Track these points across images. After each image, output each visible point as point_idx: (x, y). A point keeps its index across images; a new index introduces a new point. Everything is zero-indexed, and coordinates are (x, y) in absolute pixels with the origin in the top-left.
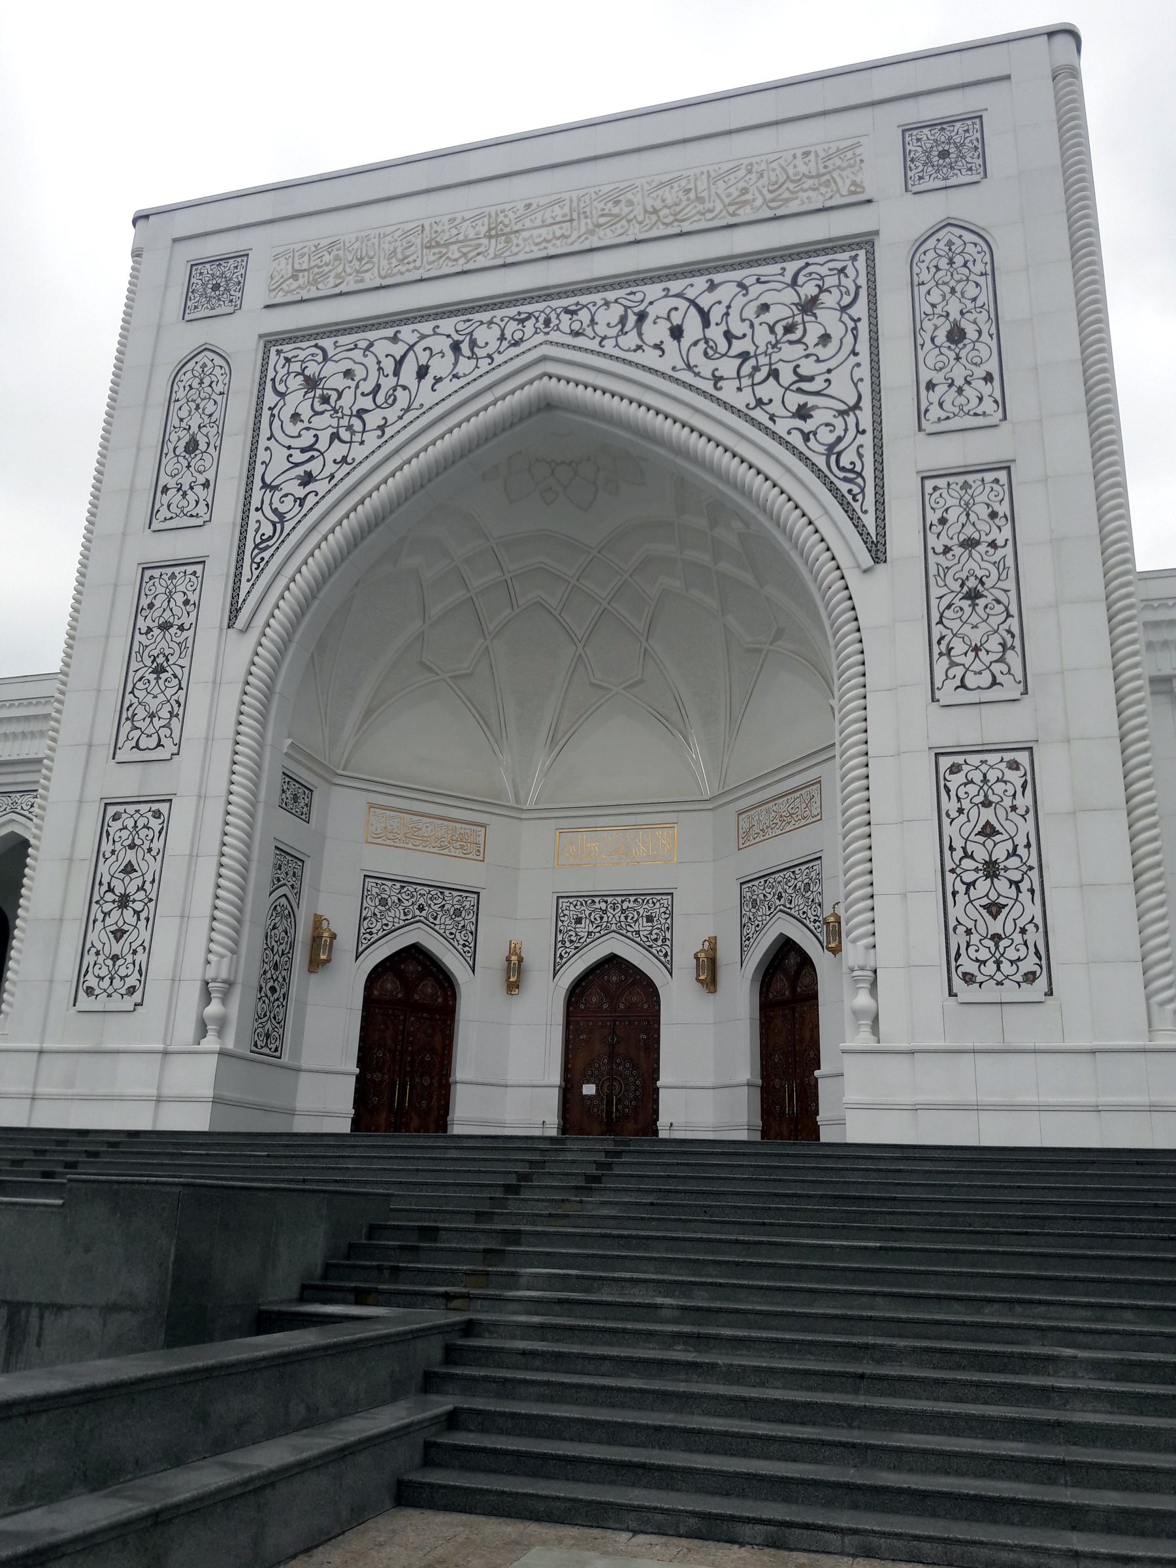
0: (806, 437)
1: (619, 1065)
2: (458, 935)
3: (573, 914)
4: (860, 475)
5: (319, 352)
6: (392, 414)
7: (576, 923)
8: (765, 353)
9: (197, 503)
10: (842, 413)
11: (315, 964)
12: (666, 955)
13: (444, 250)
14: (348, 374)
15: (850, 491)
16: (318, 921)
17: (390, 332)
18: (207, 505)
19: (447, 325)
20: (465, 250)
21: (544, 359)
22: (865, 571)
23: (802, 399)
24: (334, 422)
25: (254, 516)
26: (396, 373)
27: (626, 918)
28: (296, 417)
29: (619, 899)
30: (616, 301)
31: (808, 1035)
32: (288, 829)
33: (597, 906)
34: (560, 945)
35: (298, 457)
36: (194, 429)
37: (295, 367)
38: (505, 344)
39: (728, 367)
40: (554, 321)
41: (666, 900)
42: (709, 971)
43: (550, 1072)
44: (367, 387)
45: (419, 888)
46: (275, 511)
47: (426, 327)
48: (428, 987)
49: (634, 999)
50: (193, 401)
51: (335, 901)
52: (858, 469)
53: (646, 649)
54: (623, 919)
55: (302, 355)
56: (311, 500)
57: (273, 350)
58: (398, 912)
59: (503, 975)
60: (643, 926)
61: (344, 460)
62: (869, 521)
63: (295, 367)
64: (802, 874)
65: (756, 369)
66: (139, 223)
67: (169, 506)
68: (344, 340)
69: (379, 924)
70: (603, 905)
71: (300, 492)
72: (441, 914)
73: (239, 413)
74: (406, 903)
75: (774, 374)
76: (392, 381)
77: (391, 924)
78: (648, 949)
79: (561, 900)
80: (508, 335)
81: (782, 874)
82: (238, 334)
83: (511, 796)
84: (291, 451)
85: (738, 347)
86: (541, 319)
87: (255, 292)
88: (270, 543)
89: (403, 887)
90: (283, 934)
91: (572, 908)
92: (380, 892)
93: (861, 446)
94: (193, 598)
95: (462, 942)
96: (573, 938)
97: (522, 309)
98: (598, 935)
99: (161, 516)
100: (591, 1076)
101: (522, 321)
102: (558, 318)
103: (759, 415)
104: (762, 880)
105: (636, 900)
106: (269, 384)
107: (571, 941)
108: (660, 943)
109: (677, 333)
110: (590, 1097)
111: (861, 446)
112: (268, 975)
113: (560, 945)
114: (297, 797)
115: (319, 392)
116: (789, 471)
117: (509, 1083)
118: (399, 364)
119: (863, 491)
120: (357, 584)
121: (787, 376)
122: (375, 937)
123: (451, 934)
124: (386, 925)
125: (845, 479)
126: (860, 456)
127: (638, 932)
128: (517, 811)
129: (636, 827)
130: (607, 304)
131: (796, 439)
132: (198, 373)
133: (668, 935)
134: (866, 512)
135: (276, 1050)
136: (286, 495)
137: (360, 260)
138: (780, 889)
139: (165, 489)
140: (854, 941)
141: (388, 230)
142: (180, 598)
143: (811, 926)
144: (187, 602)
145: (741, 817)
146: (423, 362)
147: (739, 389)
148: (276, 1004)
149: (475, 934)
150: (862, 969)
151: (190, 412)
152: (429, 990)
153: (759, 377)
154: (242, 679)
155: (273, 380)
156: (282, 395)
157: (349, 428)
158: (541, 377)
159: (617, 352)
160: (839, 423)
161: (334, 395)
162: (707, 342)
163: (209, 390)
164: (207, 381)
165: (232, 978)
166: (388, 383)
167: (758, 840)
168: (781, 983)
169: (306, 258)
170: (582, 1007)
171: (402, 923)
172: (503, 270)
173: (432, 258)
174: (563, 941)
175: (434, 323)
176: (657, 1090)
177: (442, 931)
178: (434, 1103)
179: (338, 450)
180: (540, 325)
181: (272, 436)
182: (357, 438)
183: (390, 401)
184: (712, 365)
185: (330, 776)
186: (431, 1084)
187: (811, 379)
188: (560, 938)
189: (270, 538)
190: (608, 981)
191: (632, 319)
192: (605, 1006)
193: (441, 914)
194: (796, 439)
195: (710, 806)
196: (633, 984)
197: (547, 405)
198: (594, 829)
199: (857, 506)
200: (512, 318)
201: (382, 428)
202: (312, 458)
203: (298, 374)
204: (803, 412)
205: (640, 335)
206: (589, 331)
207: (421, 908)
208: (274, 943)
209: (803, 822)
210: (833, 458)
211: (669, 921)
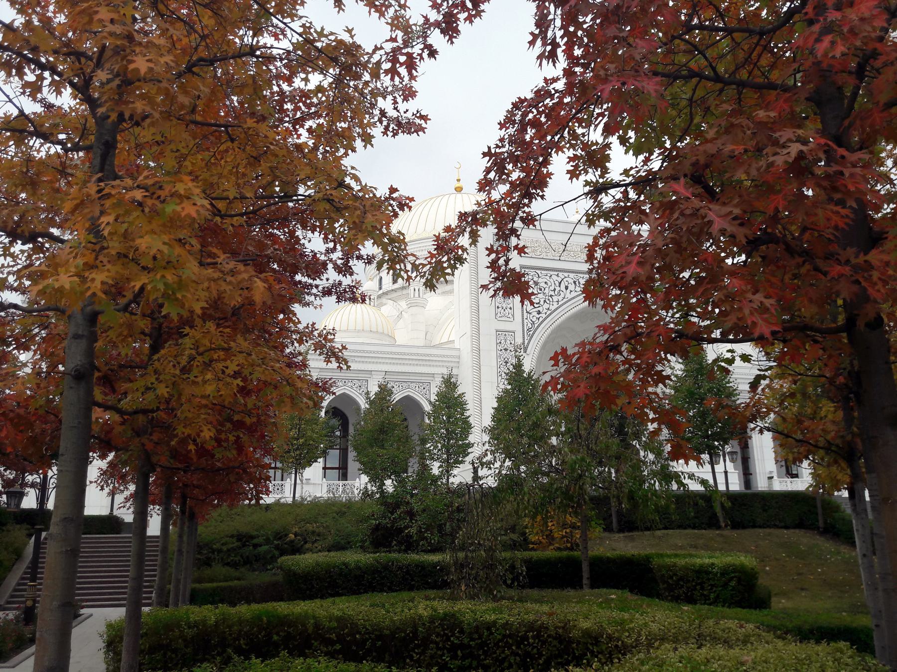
6: (560, 298)
19: (572, 275)
25: (526, 321)
47: (566, 275)
56: (541, 319)
118: (560, 283)
179: (546, 306)
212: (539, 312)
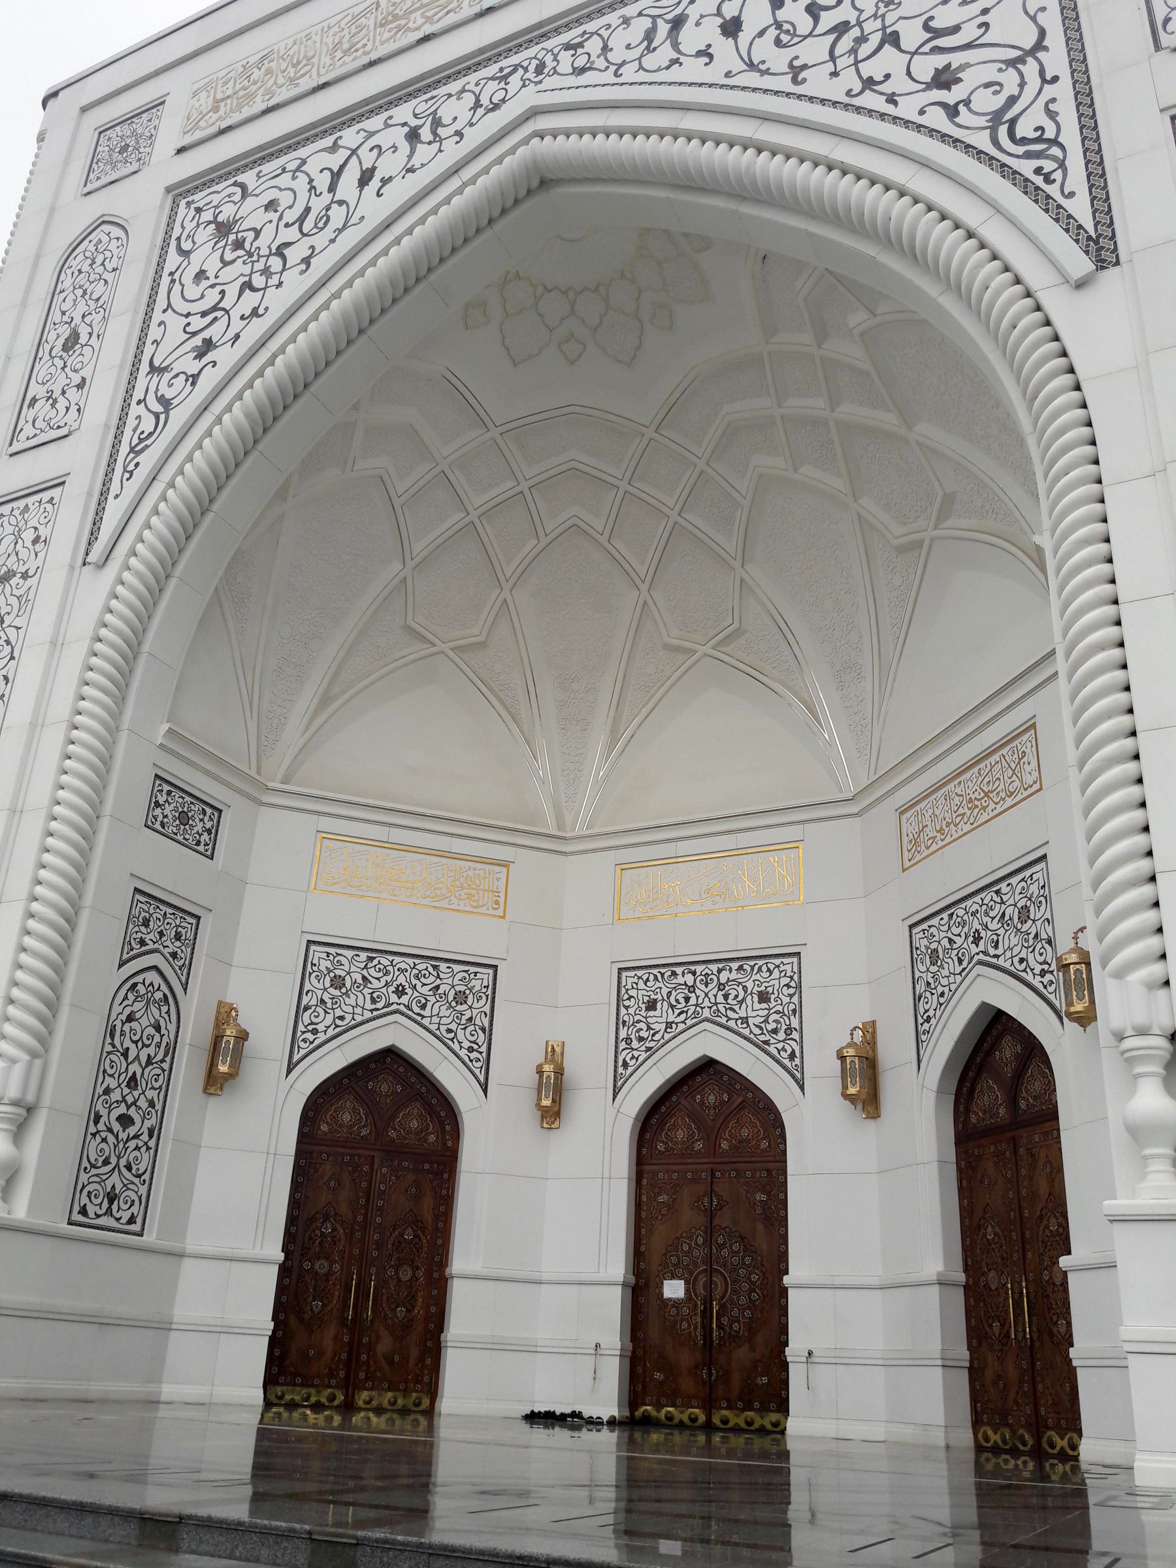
0: (952, 111)
1: (721, 1247)
2: (460, 1033)
3: (642, 994)
4: (1055, 142)
5: (238, 190)
6: (320, 240)
7: (648, 1009)
8: (875, 16)
9: (68, 409)
10: (1012, 63)
11: (213, 1082)
12: (792, 1056)
13: (403, 22)
14: (271, 206)
15: (1038, 171)
16: (225, 1014)
17: (328, 141)
18: (79, 410)
19: (403, 113)
20: (429, 14)
21: (534, 113)
22: (1080, 285)
23: (940, 61)
24: (247, 269)
25: (135, 410)
26: (332, 188)
27: (726, 997)
28: (201, 275)
29: (714, 967)
30: (640, 14)
31: (1043, 1189)
32: (170, 867)
33: (680, 980)
34: (623, 1045)
35: (197, 323)
36: (77, 320)
37: (207, 216)
38: (480, 111)
39: (814, 50)
40: (550, 64)
41: (789, 965)
44: (291, 216)
45: (397, 959)
46: (162, 400)
48: (413, 1120)
49: (745, 1133)
50: (80, 287)
51: (252, 976)
52: (1050, 133)
53: (742, 580)
54: (720, 999)
55: (216, 199)
57: (183, 203)
58: (362, 998)
59: (529, 1097)
60: (754, 1010)
61: (255, 313)
62: (1081, 209)
63: (207, 216)
64: (1013, 893)
65: (862, 39)
66: (50, 104)
67: (34, 422)
68: (267, 168)
69: (330, 1018)
70: (689, 979)
71: (193, 367)
72: (432, 999)
74: (376, 984)
75: (893, 39)
76: (327, 198)
77: (348, 1017)
78: (763, 1046)
79: (624, 974)
80: (485, 100)
81: (977, 899)
83: (550, 819)
84: (190, 319)
85: (828, 20)
86: (532, 68)
88: (148, 442)
89: (371, 959)
90: (152, 1031)
91: (641, 985)
92: (329, 968)
93: (1054, 100)
94: (43, 532)
95: (466, 1044)
96: (644, 1034)
97: (504, 63)
98: (681, 1027)
99: (22, 437)
100: (676, 1265)
101: (504, 78)
102: (555, 59)
103: (871, 100)
104: (945, 915)
105: (740, 968)
106: (173, 243)
107: (641, 1039)
108: (781, 1035)
110: (676, 1303)
111: (1054, 100)
112: (116, 1096)
113: (623, 1045)
114: (185, 816)
115: (232, 237)
116: (925, 164)
117: (545, 1277)
118: (336, 176)
119: (1062, 165)
120: (281, 495)
121: (912, 35)
122: (322, 1037)
123: (449, 1031)
124: (342, 1018)
125: (1028, 155)
126: (1052, 115)
127: (745, 1020)
128: (556, 842)
129: (739, 852)
130: (626, 21)
131: (937, 119)
133: (795, 1023)
134: (1071, 195)
135: (132, 1220)
136: (177, 376)
137: (294, 66)
138: (976, 925)
139: (34, 400)
140: (1119, 974)
141: (333, 21)
142: (28, 536)
143: (1036, 982)
144: (36, 541)
145: (904, 818)
146: (367, 165)
147: (835, 74)
148: (132, 1144)
149: (488, 1032)
150: (1142, 1032)
151: (75, 301)
152: (414, 1124)
153: (865, 50)
154: (90, 633)
155: (178, 239)
156: (185, 254)
157: (266, 272)
158: (526, 141)
159: (643, 76)
160: (1010, 79)
161: (251, 235)
162: (778, 25)
163: (100, 270)
164: (99, 260)
165: (30, 1098)
166: (317, 205)
167: (934, 847)
168: (991, 1097)
169: (230, 85)
170: (661, 1147)
171: (368, 1015)
172: (481, 21)
173: (387, 35)
174: (628, 1040)
175: (386, 115)
176: (784, 1292)
177: (433, 1027)
178: (419, 1311)
180: (531, 75)
181: (169, 305)
182: (275, 280)
183: (321, 225)
184: (787, 54)
185: (257, 793)
186: (414, 1278)
187: (956, 29)
188: (623, 1034)
189: (151, 434)
190: (702, 1103)
191: (663, 28)
192: (699, 1146)
193: (432, 999)
194: (937, 119)
195: (855, 809)
196: (741, 1106)
197: (541, 181)
198: (675, 860)
199: (1053, 190)
200: (493, 78)
201: (307, 261)
202: (216, 319)
203: (210, 223)
204: (944, 77)
205: (676, 46)
206: (600, 63)
207: (400, 991)
208: (127, 1043)
209: (1009, 802)
210: (1003, 130)
211: (795, 999)
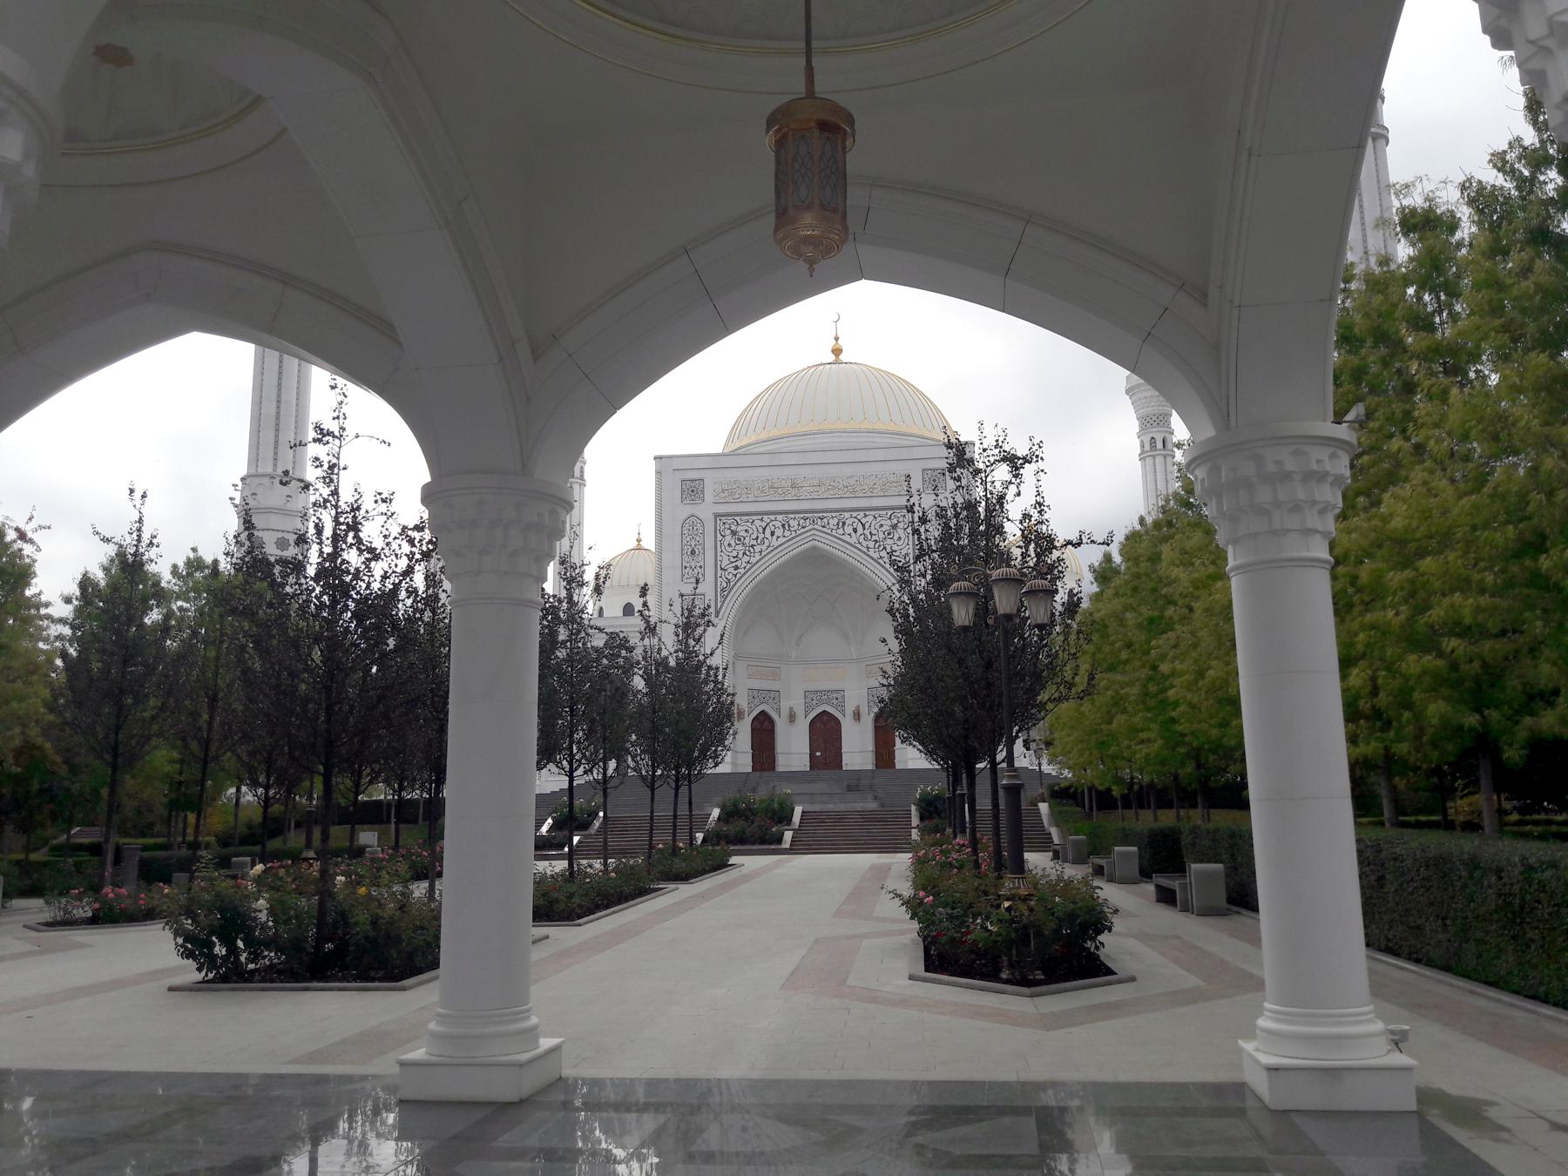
19: (780, 517)
39: (871, 544)
42: (857, 716)
43: (805, 748)
73: (709, 543)
82: (706, 510)
87: (709, 495)
109: (855, 530)
132: (691, 526)
179: (746, 559)
197: (814, 548)
212: (736, 568)
